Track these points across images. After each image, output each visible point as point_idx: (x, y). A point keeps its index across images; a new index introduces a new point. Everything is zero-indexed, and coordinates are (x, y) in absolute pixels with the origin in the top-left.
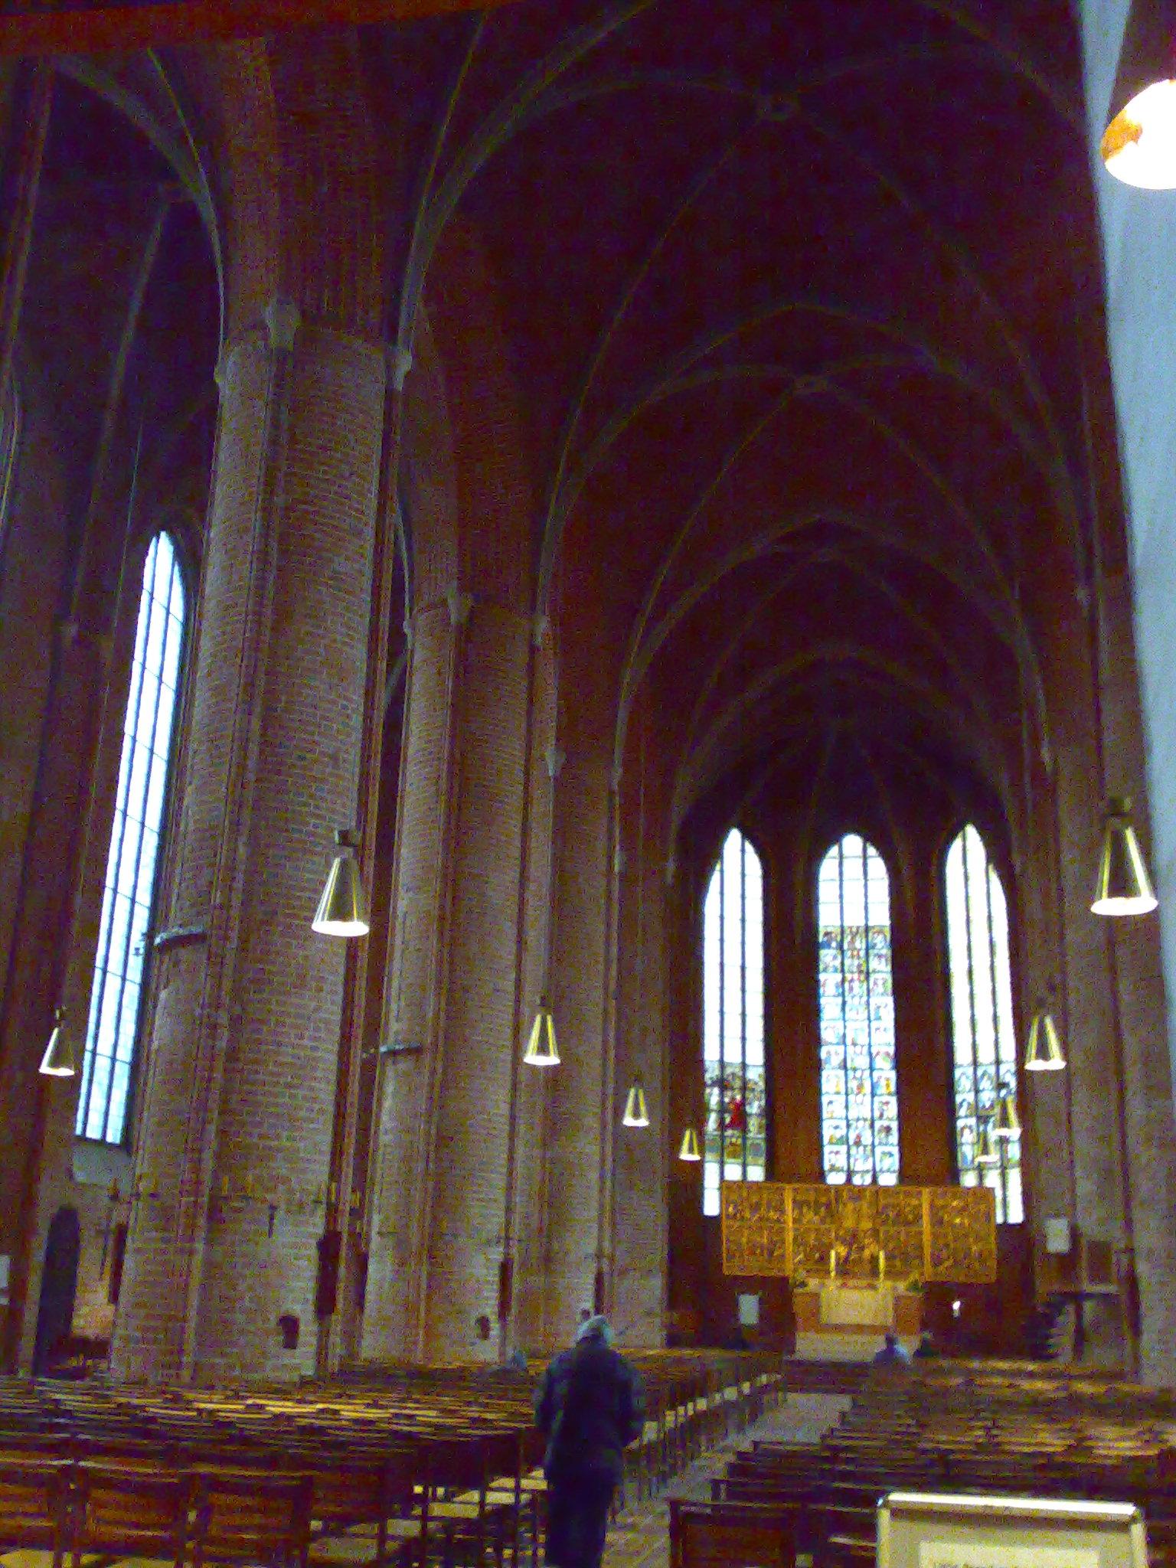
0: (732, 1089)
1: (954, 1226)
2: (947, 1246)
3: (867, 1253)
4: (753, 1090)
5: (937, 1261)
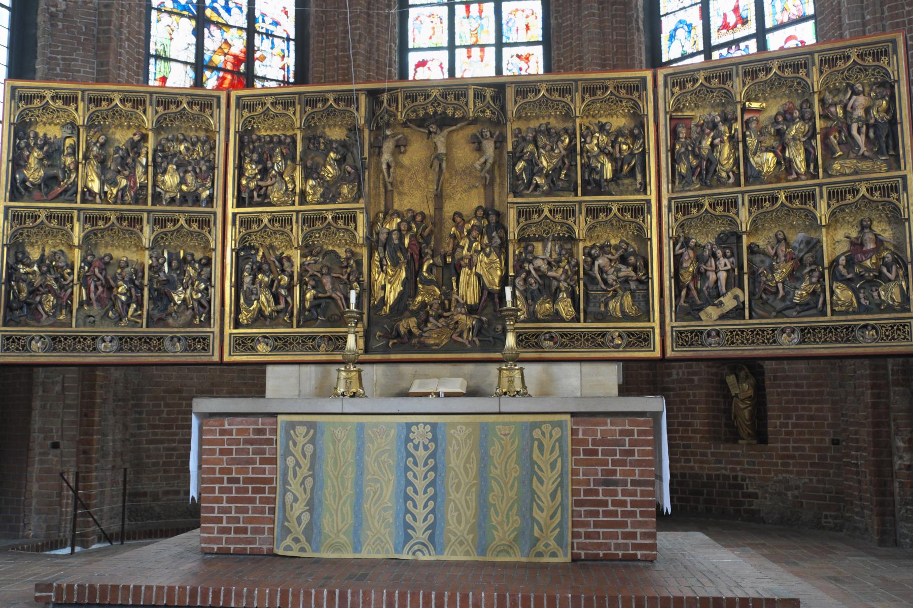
0: (223, 26)
1: (754, 176)
2: (730, 240)
3: (467, 290)
4: (269, 35)
5: (691, 299)
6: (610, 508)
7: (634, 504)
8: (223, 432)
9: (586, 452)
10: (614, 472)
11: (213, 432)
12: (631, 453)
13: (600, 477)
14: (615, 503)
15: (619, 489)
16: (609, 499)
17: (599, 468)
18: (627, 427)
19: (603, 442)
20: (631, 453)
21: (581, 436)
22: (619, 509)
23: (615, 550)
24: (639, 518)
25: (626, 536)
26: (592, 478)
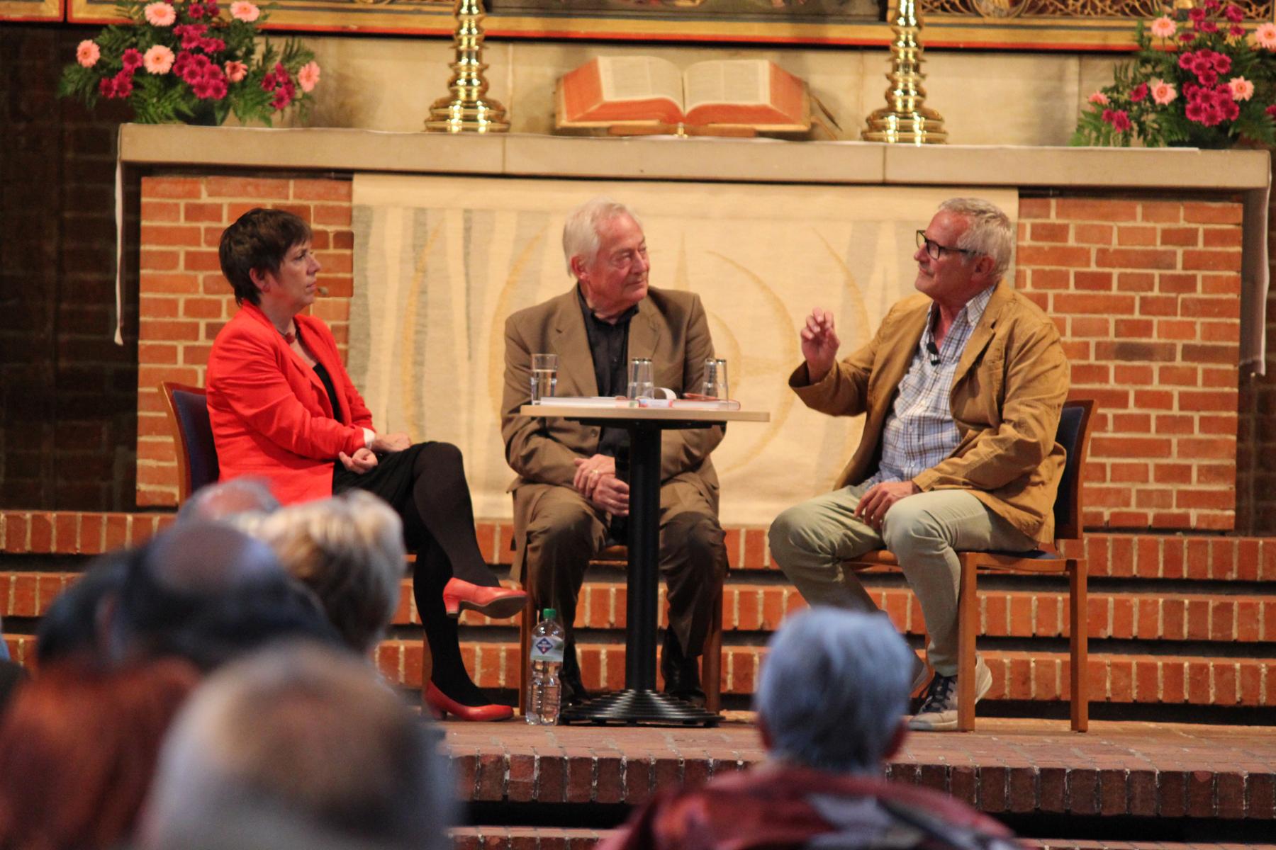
6: (1132, 409)
7: (1188, 402)
8: (195, 212)
9: (1082, 280)
10: (1146, 329)
11: (171, 211)
12: (1186, 284)
13: (1111, 337)
14: (1142, 399)
15: (1156, 366)
16: (1131, 390)
17: (1112, 319)
18: (1183, 224)
19: (1124, 258)
20: (1186, 284)
21: (1071, 242)
22: (1154, 413)
23: (1140, 504)
24: (1197, 434)
25: (1167, 474)
26: (1093, 341)
